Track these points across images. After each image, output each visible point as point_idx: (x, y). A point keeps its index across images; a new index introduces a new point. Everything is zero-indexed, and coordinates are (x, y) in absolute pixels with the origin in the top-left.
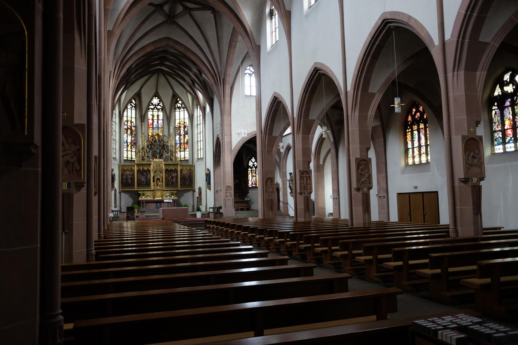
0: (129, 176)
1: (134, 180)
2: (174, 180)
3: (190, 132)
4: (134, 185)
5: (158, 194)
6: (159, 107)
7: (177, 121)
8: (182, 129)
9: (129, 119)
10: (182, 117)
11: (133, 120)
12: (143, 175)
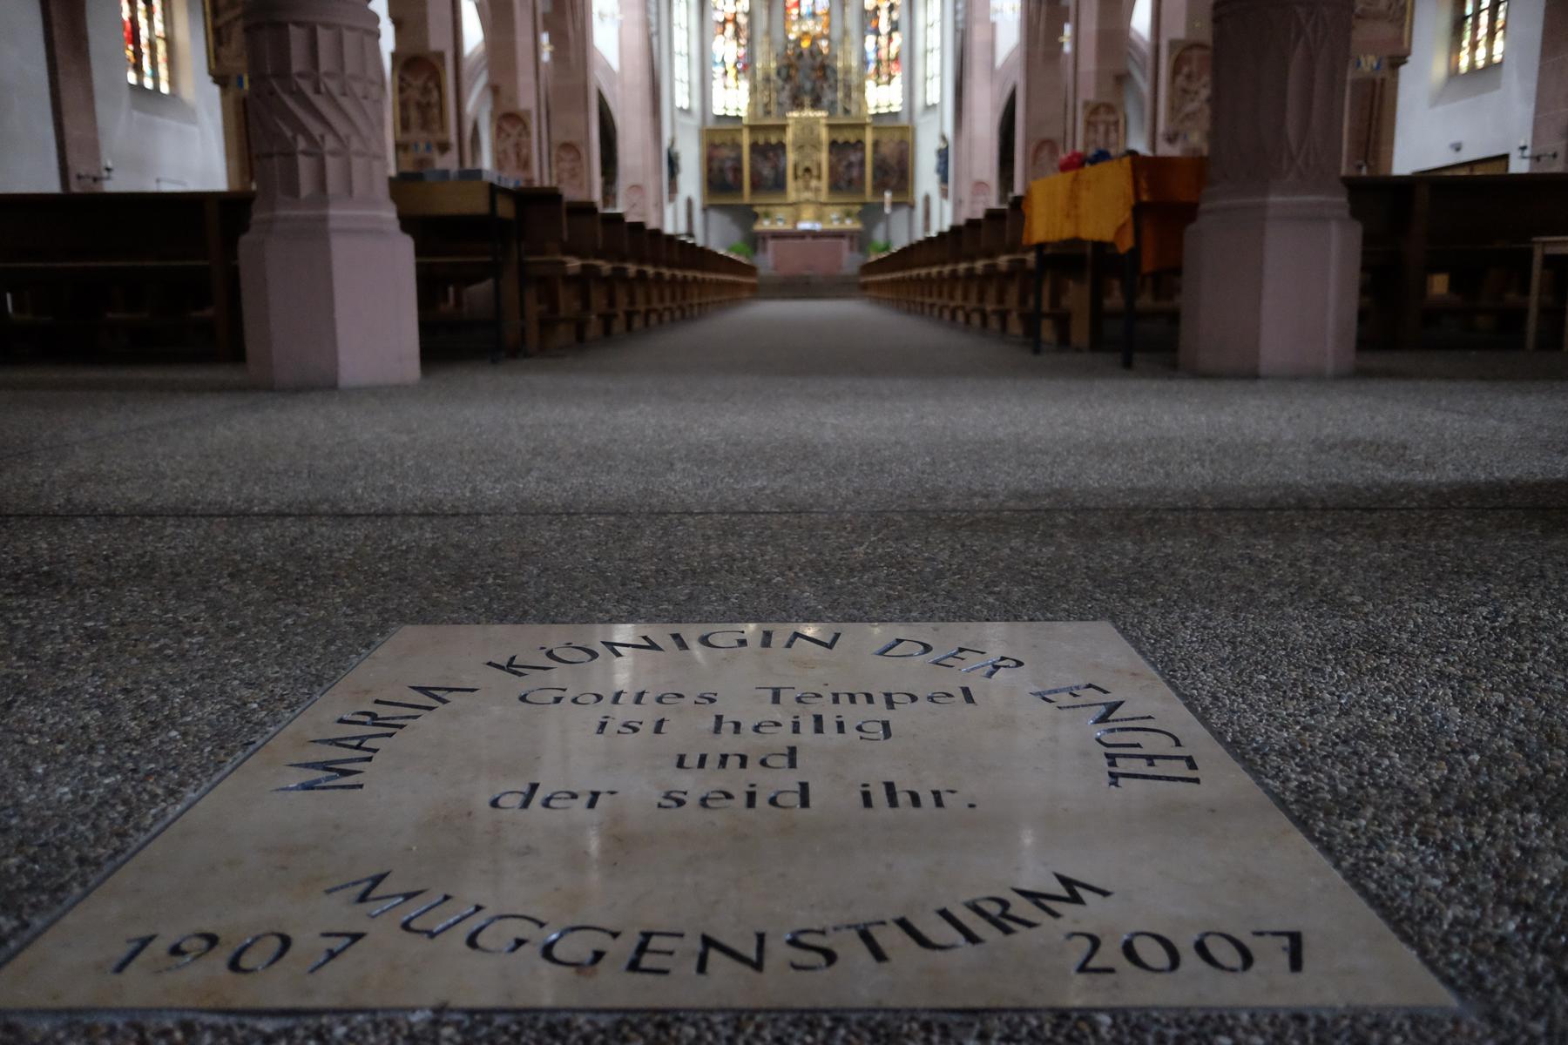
0: (729, 164)
2: (855, 173)
3: (904, 25)
12: (766, 158)
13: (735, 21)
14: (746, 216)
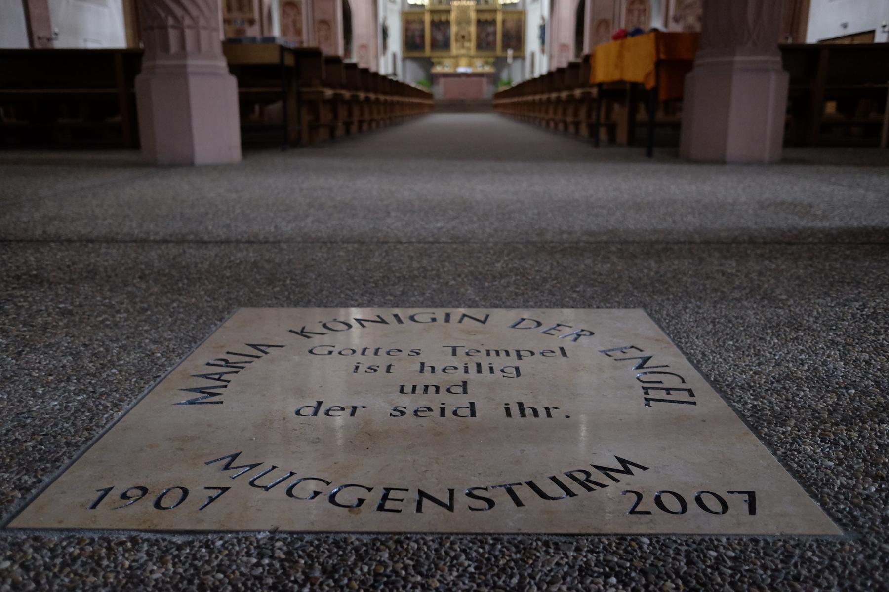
0: (417, 33)
2: (491, 38)
14: (427, 64)
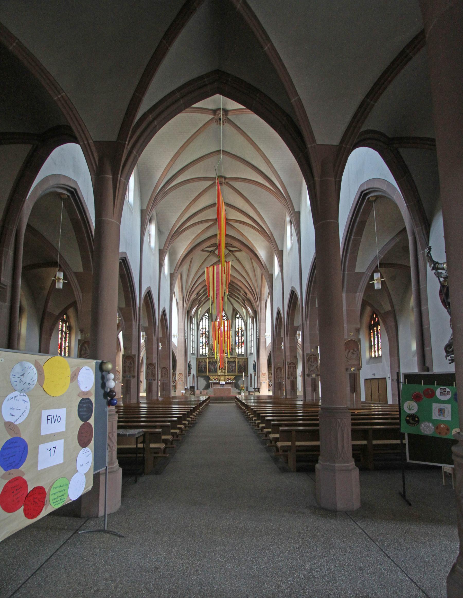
1: (205, 368)
4: (206, 372)
5: (222, 378)
6: (224, 318)
7: (237, 327)
8: (240, 332)
9: (204, 327)
10: (240, 324)
11: (207, 328)
12: (212, 364)
13: (205, 334)
